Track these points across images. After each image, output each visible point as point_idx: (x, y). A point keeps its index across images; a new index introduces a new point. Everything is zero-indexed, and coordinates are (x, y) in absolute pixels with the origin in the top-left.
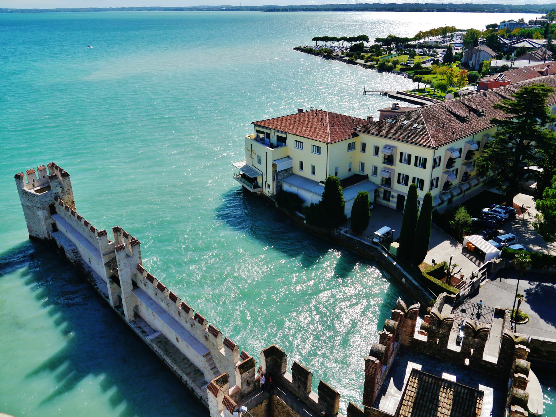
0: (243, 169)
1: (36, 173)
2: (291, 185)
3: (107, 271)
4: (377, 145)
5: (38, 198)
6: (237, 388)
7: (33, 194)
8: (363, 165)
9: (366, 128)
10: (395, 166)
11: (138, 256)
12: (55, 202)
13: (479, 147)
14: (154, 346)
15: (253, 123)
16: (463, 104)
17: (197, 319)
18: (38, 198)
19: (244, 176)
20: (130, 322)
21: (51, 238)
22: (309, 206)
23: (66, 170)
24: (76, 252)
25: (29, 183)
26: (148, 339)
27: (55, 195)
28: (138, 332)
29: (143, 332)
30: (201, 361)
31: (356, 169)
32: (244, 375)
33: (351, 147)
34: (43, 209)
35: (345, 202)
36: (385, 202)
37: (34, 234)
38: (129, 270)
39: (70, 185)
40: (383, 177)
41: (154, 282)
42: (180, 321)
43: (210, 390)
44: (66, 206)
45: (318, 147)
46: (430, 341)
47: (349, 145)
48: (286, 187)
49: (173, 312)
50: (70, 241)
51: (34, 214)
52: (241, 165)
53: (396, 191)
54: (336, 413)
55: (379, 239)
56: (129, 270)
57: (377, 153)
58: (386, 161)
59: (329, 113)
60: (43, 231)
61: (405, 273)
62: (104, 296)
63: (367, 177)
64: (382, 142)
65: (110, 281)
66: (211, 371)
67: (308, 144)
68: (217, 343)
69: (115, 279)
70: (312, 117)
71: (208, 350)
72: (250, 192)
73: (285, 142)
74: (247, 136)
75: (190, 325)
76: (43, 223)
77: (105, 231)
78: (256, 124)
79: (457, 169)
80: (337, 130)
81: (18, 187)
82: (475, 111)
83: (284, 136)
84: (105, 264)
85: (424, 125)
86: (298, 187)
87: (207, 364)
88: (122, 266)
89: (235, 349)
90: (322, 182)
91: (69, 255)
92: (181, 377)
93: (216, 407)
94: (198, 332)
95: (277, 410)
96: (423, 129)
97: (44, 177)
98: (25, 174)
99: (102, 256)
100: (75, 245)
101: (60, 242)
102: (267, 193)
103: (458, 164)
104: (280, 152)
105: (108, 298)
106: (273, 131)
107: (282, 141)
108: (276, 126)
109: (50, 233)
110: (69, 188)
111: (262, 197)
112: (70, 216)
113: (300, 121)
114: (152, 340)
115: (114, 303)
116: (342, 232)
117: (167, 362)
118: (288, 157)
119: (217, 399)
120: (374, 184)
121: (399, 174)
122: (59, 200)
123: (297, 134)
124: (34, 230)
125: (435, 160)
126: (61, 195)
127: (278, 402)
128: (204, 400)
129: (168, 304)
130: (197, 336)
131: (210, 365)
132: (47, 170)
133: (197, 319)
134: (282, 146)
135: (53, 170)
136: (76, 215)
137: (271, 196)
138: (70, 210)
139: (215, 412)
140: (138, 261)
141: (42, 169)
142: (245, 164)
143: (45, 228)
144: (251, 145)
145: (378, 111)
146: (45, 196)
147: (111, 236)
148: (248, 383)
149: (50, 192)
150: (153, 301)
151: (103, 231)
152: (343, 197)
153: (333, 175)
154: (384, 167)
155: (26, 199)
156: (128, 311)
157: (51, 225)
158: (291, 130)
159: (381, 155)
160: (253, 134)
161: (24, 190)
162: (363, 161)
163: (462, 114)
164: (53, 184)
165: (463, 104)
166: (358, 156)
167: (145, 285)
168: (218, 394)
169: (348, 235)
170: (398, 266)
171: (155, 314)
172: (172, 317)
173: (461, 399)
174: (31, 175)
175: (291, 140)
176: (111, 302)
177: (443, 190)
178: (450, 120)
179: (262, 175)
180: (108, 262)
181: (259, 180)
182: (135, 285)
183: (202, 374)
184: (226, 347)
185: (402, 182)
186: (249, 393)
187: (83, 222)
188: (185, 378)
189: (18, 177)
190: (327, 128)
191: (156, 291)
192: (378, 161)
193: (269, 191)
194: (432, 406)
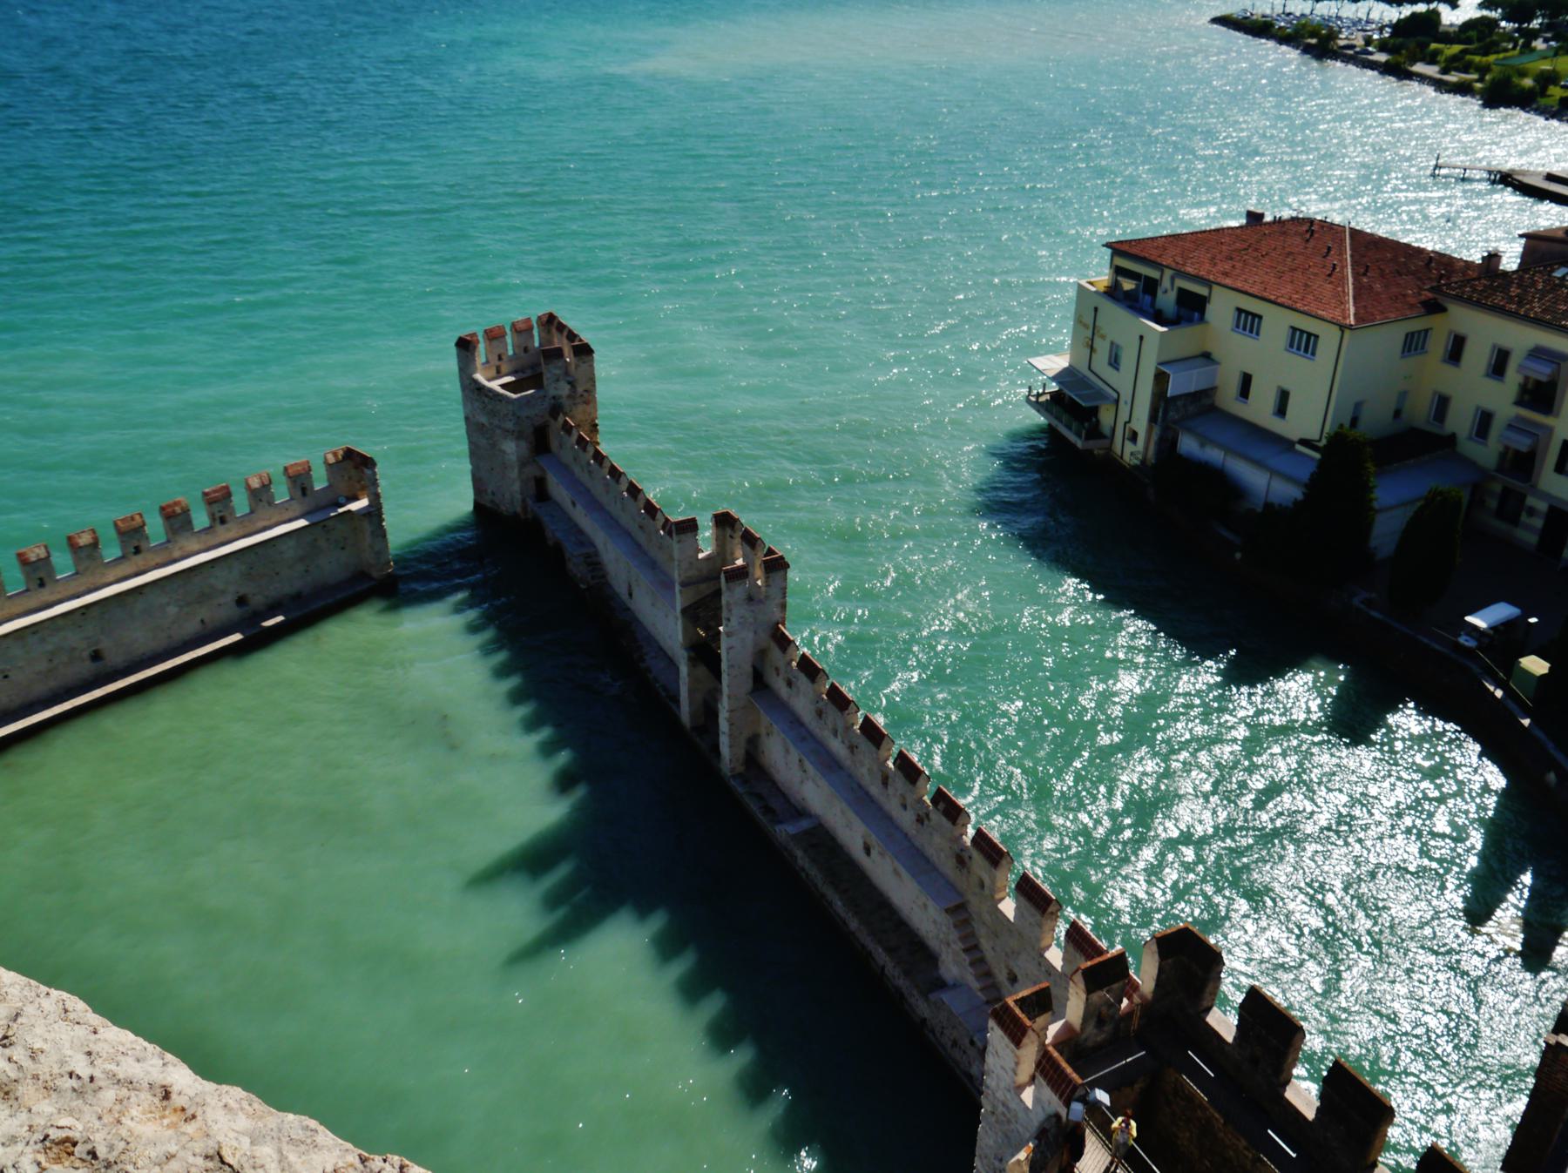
0: (1062, 377)
1: (509, 339)
2: (1204, 441)
3: (685, 630)
4: (1505, 343)
6: (1068, 1027)
7: (497, 395)
8: (1443, 403)
9: (1474, 290)
10: (1557, 415)
11: (778, 601)
12: (552, 421)
14: (799, 853)
15: (1108, 245)
17: (941, 806)
18: (510, 408)
19: (1055, 396)
21: (530, 516)
22: (1259, 510)
23: (586, 337)
24: (594, 562)
25: (487, 362)
26: (785, 831)
28: (754, 806)
29: (768, 810)
30: (935, 922)
31: (1420, 411)
32: (1095, 997)
33: (1414, 344)
34: (519, 436)
35: (1378, 511)
36: (1500, 526)
37: (486, 501)
38: (751, 635)
39: (592, 380)
40: (1507, 448)
42: (882, 799)
43: (1002, 1024)
44: (580, 436)
45: (1309, 335)
47: (1410, 337)
48: (1188, 445)
49: (864, 771)
50: (581, 532)
51: (494, 446)
52: (1054, 366)
53: (1545, 496)
54: (1369, 1163)
55: (1477, 640)
56: (749, 636)
58: (1526, 397)
59: (1354, 233)
60: (512, 492)
61: (1560, 757)
63: (1452, 439)
64: (1521, 337)
65: (690, 659)
66: (963, 956)
67: (1277, 323)
68: (993, 881)
69: (705, 654)
70: (1298, 240)
71: (961, 894)
72: (1073, 446)
73: (1202, 311)
74: (1083, 282)
75: (914, 818)
76: (514, 474)
77: (694, 520)
80: (1377, 286)
84: (684, 611)
86: (1228, 450)
87: (954, 935)
88: (734, 622)
89: (1050, 910)
90: (1305, 442)
91: (576, 567)
92: (870, 953)
93: (1011, 1073)
94: (937, 839)
97: (526, 350)
98: (481, 338)
99: (677, 588)
100: (592, 544)
101: (554, 531)
102: (1127, 457)
104: (1187, 339)
105: (676, 701)
106: (1168, 273)
107: (1191, 308)
108: (1179, 259)
109: (529, 502)
110: (588, 386)
111: (1111, 463)
112: (589, 464)
113: (1256, 250)
114: (794, 837)
115: (693, 716)
116: (1356, 601)
117: (830, 903)
118: (1207, 356)
119: (1019, 1052)
120: (1470, 464)
122: (561, 419)
123: (1246, 288)
124: (489, 491)
126: (566, 402)
127: (1180, 1089)
128: (933, 1031)
129: (852, 748)
130: (930, 851)
131: (963, 939)
132: (536, 332)
133: (941, 806)
134: (1190, 321)
135: (549, 332)
136: (606, 464)
137: (1135, 467)
138: (591, 450)
139: (1002, 1085)
140: (777, 615)
141: (522, 326)
142: (1066, 365)
143: (517, 487)
144: (1096, 309)
145: (1521, 236)
147: (706, 535)
148: (1100, 1022)
149: (542, 393)
151: (689, 520)
152: (1373, 496)
153: (1347, 425)
154: (1519, 418)
155: (477, 404)
156: (731, 747)
158: (1226, 274)
159: (1513, 377)
160: (1103, 277)
161: (476, 382)
162: (1446, 390)
164: (550, 372)
166: (1434, 373)
167: (790, 684)
168: (1025, 1041)
169: (1375, 614)
170: (1538, 733)
171: (808, 765)
172: (860, 786)
174: (495, 343)
175: (1222, 307)
176: (685, 711)
179: (1117, 402)
180: (690, 606)
181: (1106, 417)
182: (759, 682)
183: (932, 959)
184: (1022, 899)
186: (1098, 1047)
187: (624, 486)
188: (881, 956)
189: (465, 346)
190: (1344, 278)
191: (821, 704)
192: (1501, 398)
193: (1131, 453)
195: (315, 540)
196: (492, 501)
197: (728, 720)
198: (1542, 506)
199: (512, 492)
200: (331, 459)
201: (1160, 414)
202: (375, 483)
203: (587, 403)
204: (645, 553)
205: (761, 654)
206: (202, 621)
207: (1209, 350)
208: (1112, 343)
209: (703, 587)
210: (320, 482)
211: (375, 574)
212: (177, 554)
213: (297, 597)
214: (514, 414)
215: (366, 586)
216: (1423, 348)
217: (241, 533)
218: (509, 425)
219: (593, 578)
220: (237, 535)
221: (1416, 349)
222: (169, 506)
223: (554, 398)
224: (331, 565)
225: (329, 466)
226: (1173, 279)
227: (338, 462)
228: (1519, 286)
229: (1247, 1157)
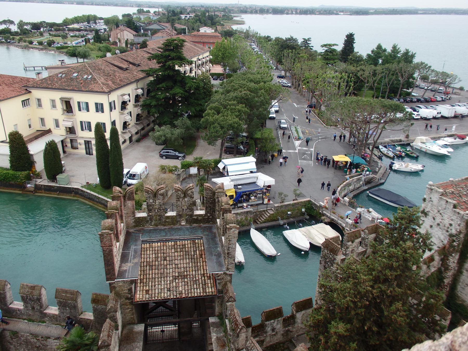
8: (42, 120)
13: (143, 92)
16: (122, 59)
31: (37, 126)
33: (25, 103)
46: (150, 214)
57: (54, 106)
64: (57, 95)
79: (131, 112)
82: (134, 64)
85: (92, 76)
95: (12, 346)
96: (93, 79)
103: (130, 107)
121: (81, 122)
125: (110, 104)
162: (42, 117)
163: (124, 66)
165: (122, 59)
173: (187, 249)
177: (123, 130)
178: (114, 71)
185: (86, 129)
194: (167, 262)
198: (82, 141)
221: (27, 106)
228: (50, 81)
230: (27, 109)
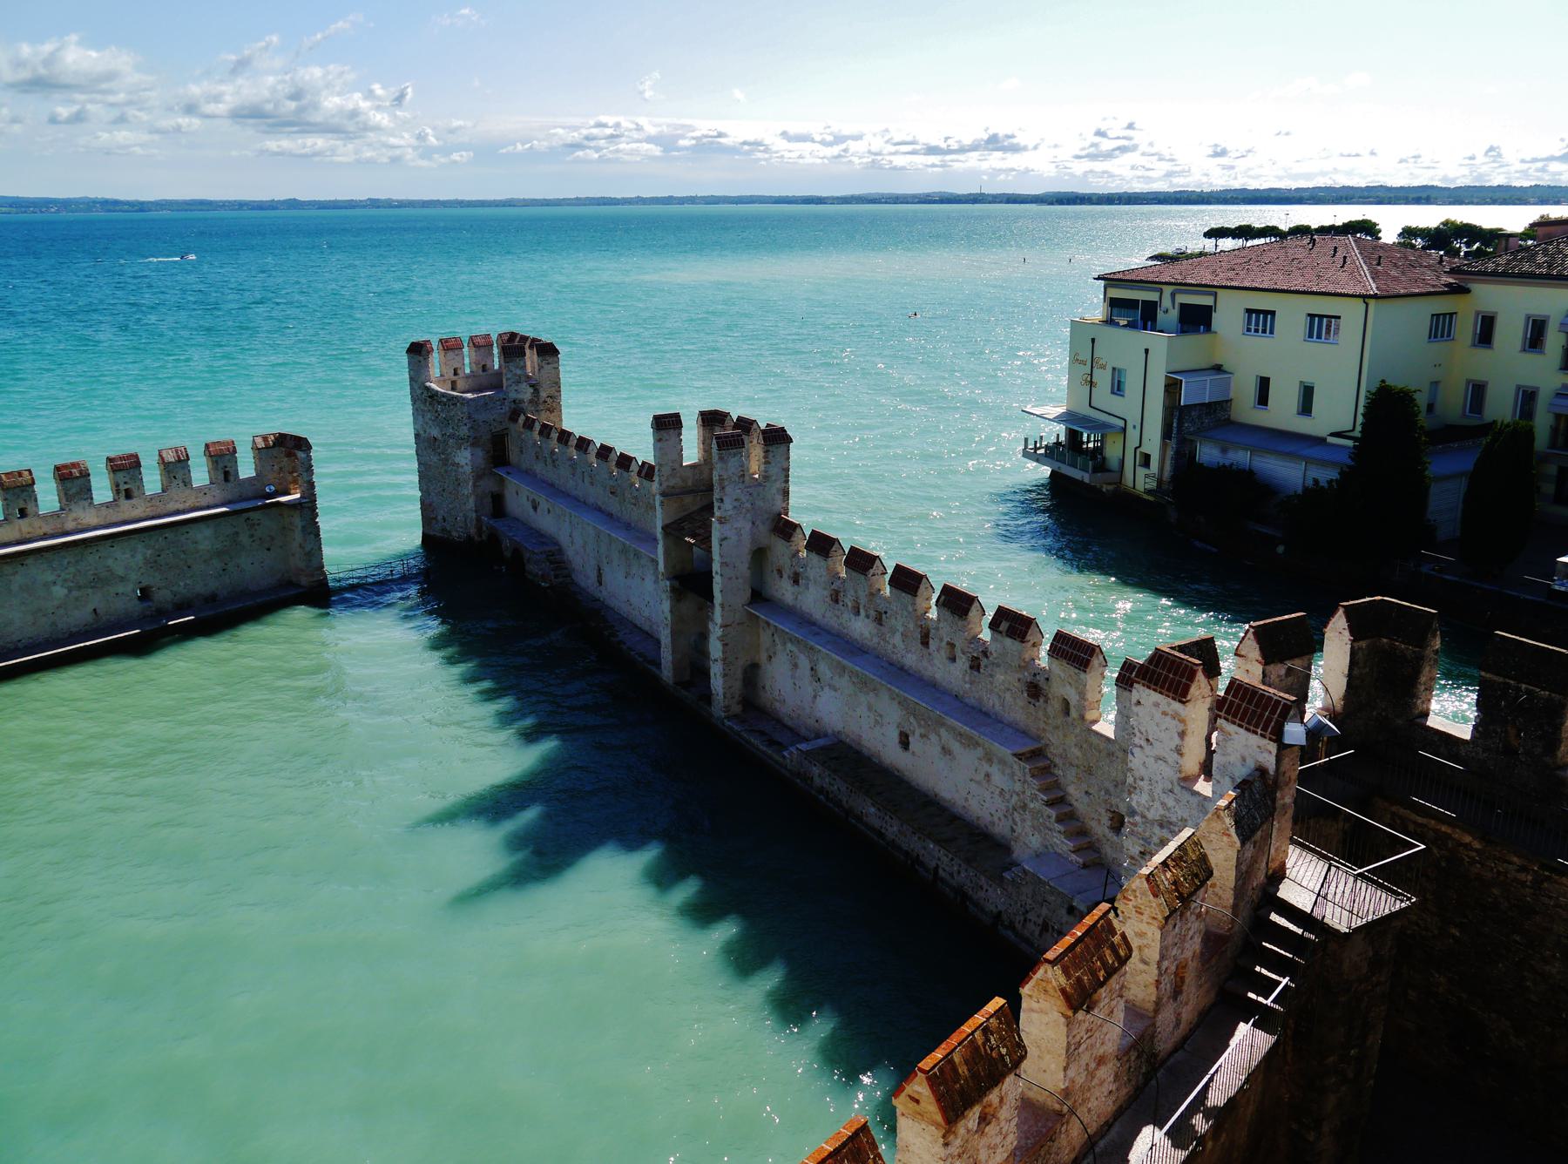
1: (466, 350)
5: (465, 409)
8: (1478, 391)
11: (779, 485)
18: (465, 409)
20: (728, 718)
26: (791, 755)
27: (513, 406)
29: (772, 742)
33: (1441, 327)
37: (436, 532)
39: (557, 384)
41: (832, 553)
48: (1208, 453)
51: (445, 462)
62: (641, 659)
65: (673, 589)
68: (1082, 695)
72: (1081, 483)
76: (468, 489)
77: (677, 416)
78: (1110, 280)
81: (412, 379)
83: (1206, 301)
88: (728, 504)
97: (484, 368)
100: (556, 543)
102: (1140, 487)
104: (1194, 349)
105: (659, 665)
107: (1196, 319)
110: (552, 391)
118: (1218, 369)
124: (440, 518)
128: (1012, 927)
130: (992, 702)
133: (1004, 626)
140: (779, 504)
141: (482, 342)
143: (471, 503)
146: (484, 404)
150: (819, 627)
156: (725, 675)
157: (490, 500)
161: (428, 389)
162: (1479, 377)
174: (450, 354)
175: (1229, 315)
176: (667, 673)
179: (1124, 430)
181: (1113, 451)
189: (418, 350)
193: (1141, 481)
195: (237, 533)
196: (444, 530)
197: (721, 639)
199: (466, 506)
200: (261, 444)
201: (1175, 425)
202: (309, 469)
203: (551, 411)
204: (618, 520)
205: (759, 555)
206: (95, 610)
207: (1219, 362)
208: (1114, 369)
209: (688, 499)
210: (246, 468)
211: (304, 581)
212: (70, 525)
213: (212, 599)
214: (469, 418)
215: (292, 592)
216: (1449, 335)
217: (151, 514)
218: (464, 431)
219: (556, 576)
220: (143, 515)
221: (1442, 336)
222: (65, 466)
223: (514, 401)
224: (253, 567)
225: (255, 448)
226: (1173, 295)
227: (267, 447)
229: (1523, 883)
230: (1440, 347)
